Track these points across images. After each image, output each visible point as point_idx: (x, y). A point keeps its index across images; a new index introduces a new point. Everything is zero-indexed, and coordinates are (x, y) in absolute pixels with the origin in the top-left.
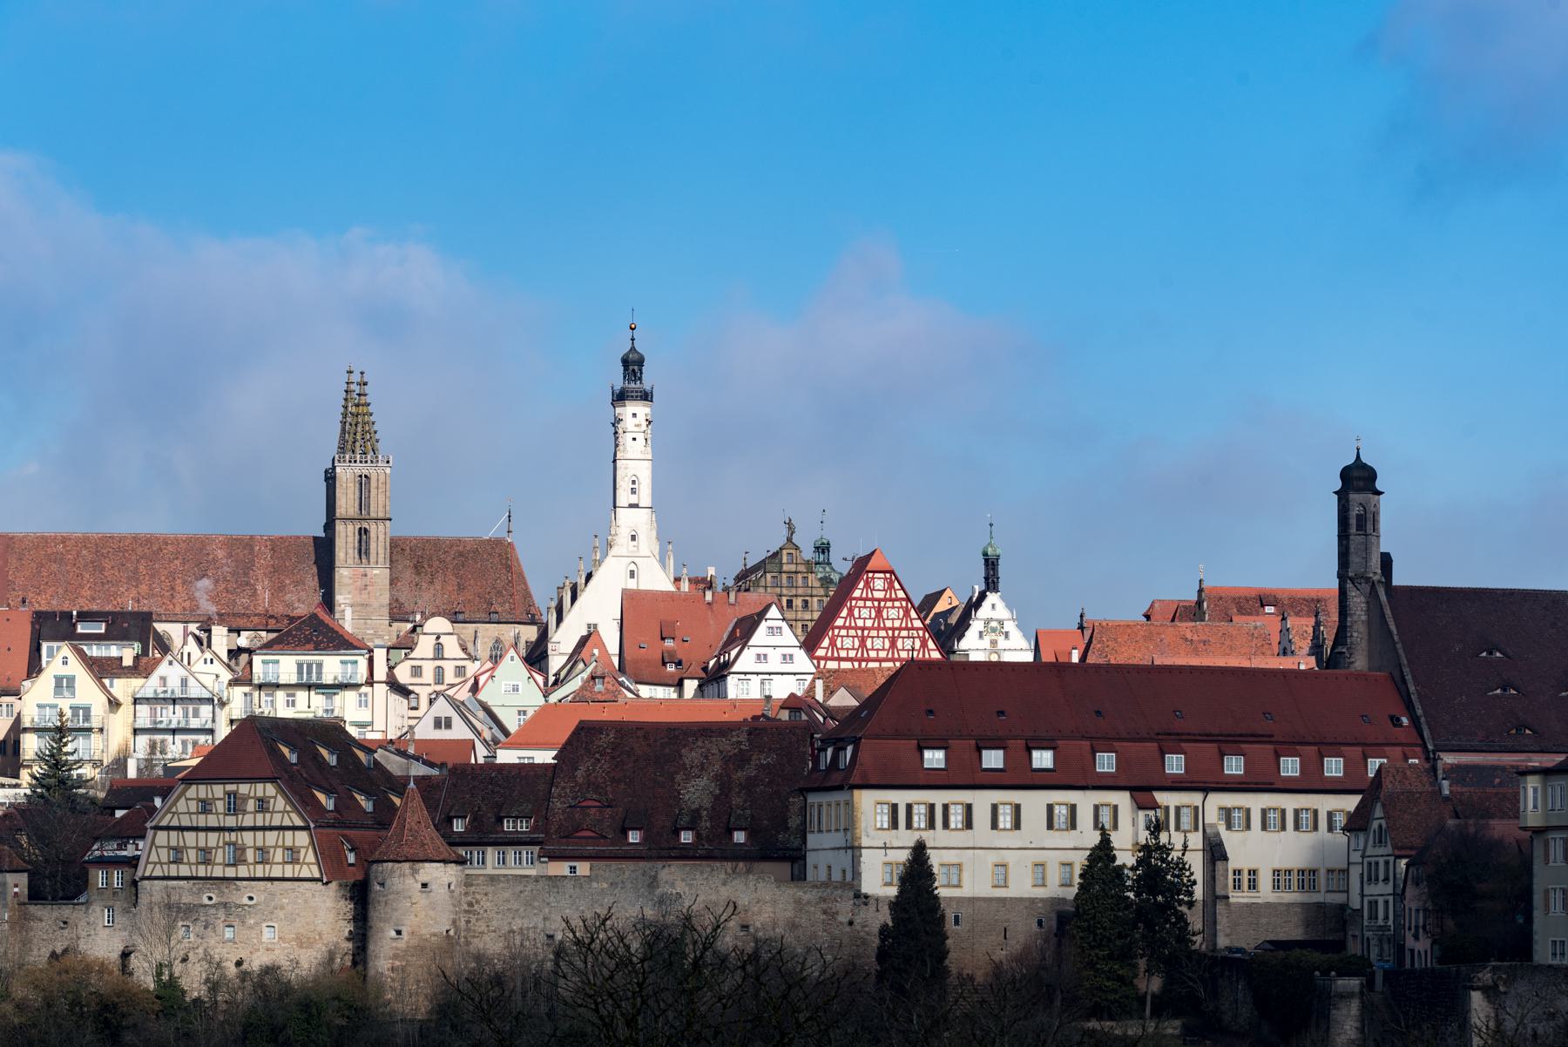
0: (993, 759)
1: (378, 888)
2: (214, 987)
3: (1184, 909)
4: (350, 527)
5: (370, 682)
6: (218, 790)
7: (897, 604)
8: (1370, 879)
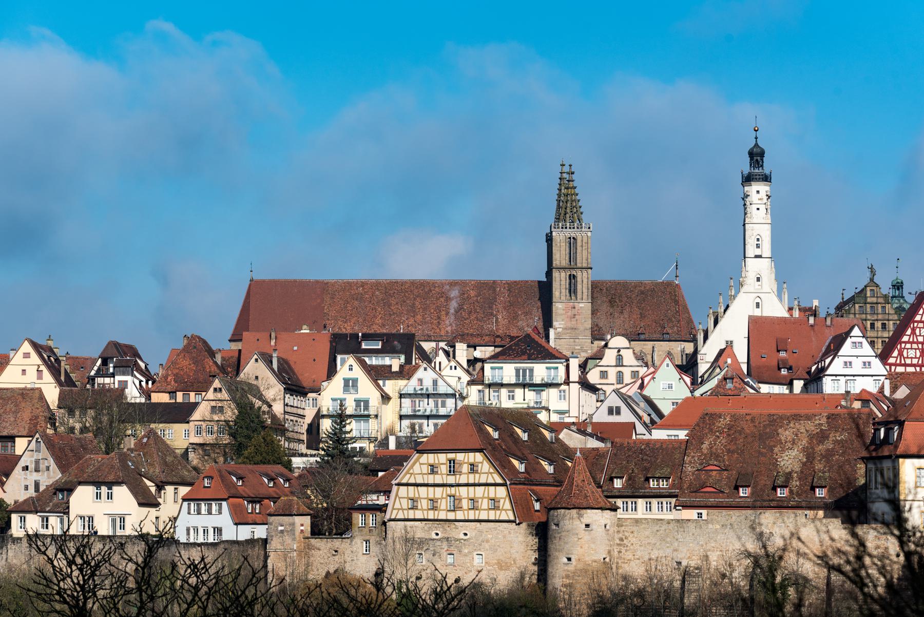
1: (554, 527)
4: (563, 274)
5: (567, 382)
6: (443, 458)
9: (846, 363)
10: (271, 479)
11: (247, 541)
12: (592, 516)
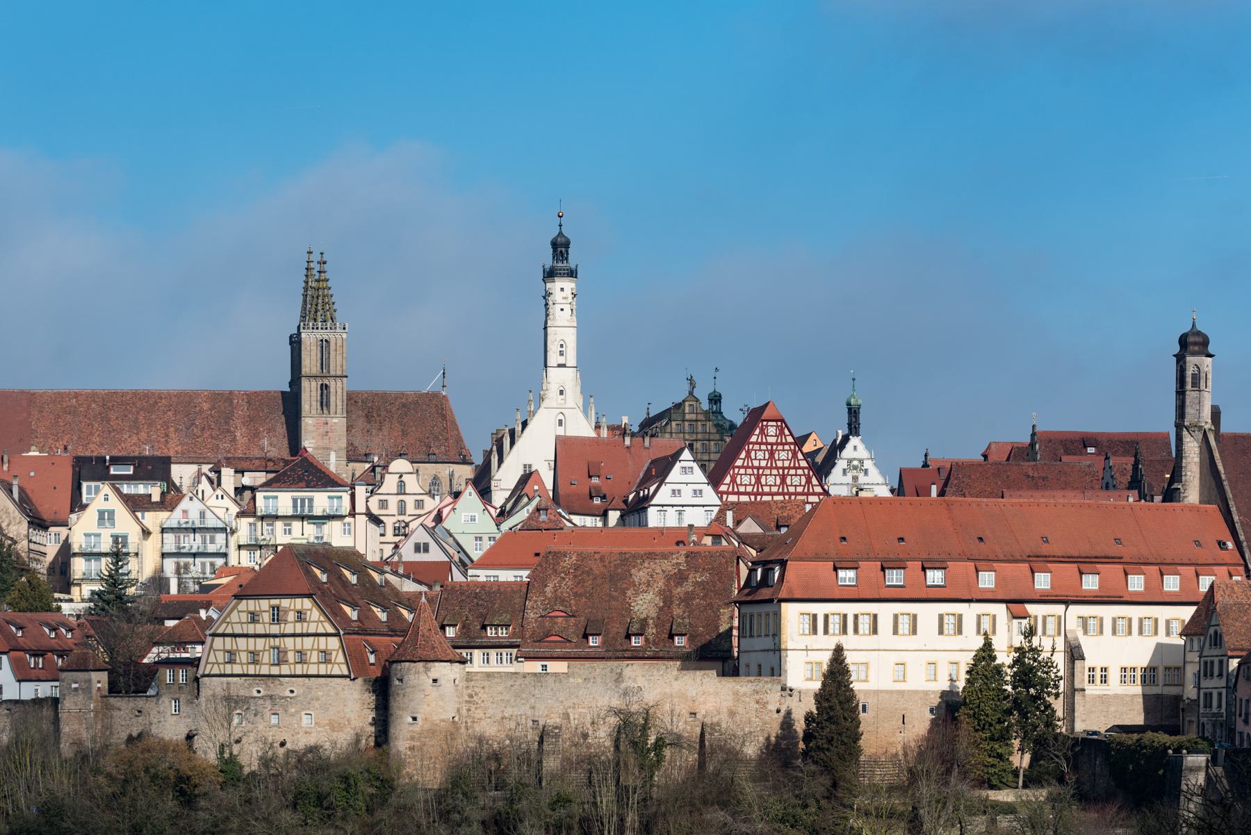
0: (895, 577)
1: (397, 683)
2: (266, 762)
3: (1051, 699)
4: (314, 384)
5: (353, 514)
6: (265, 604)
7: (787, 447)
8: (1205, 675)
9: (674, 491)
10: (53, 629)
11: (33, 700)
12: (439, 669)
